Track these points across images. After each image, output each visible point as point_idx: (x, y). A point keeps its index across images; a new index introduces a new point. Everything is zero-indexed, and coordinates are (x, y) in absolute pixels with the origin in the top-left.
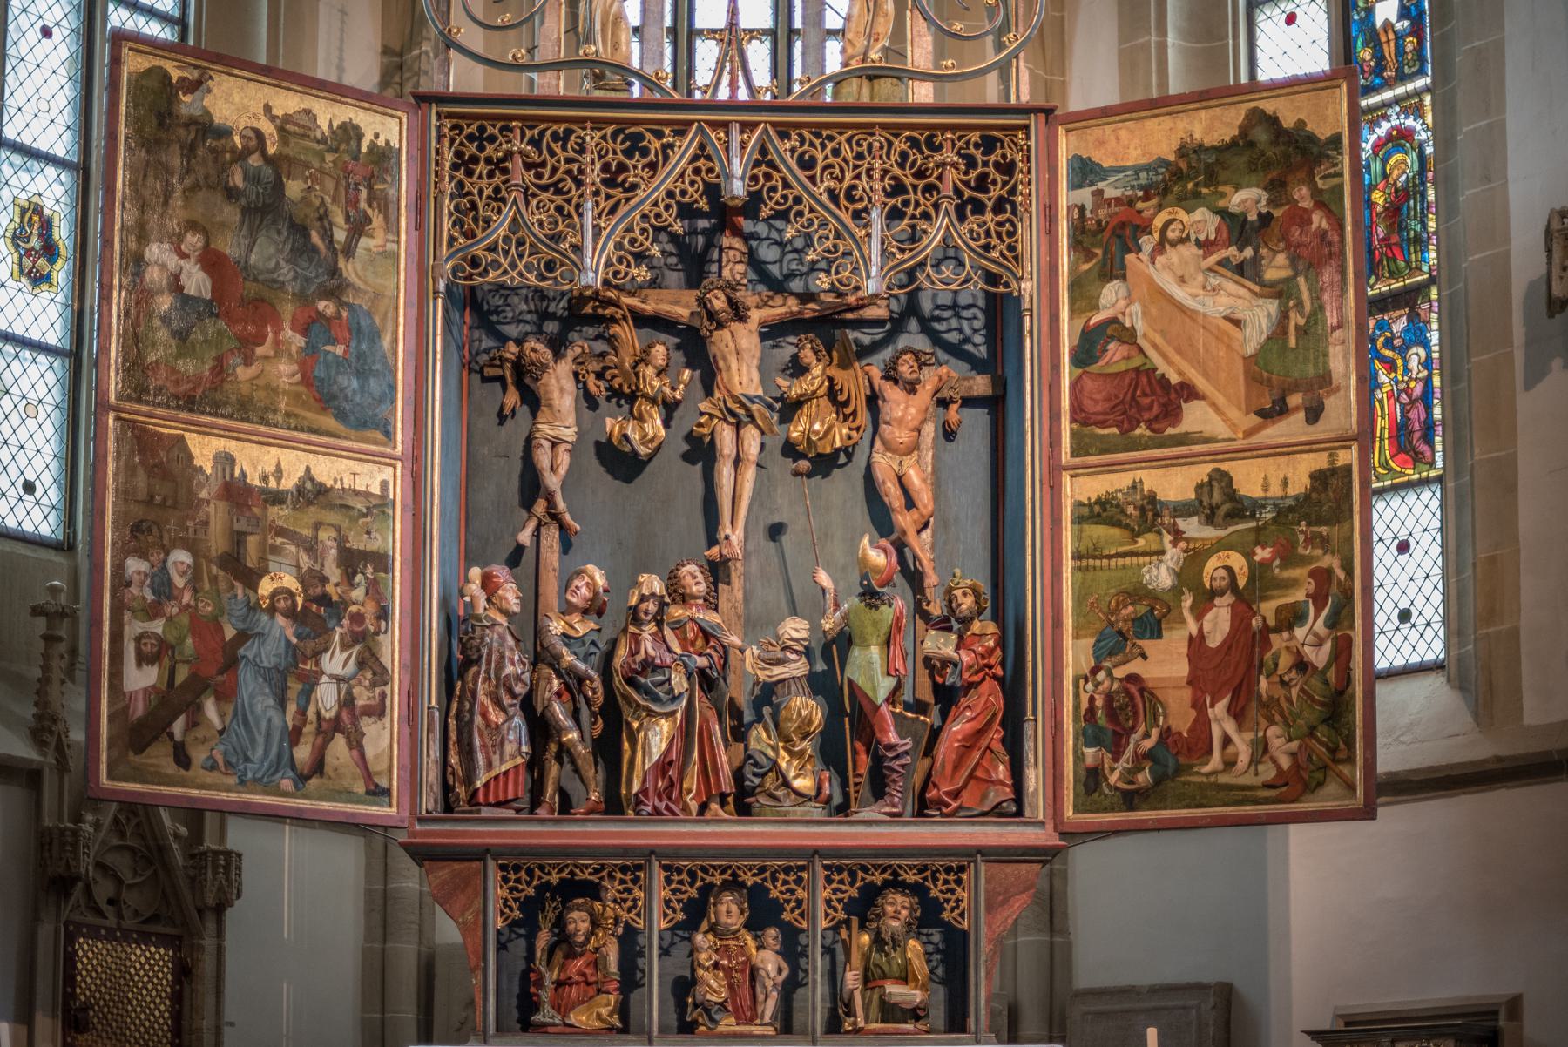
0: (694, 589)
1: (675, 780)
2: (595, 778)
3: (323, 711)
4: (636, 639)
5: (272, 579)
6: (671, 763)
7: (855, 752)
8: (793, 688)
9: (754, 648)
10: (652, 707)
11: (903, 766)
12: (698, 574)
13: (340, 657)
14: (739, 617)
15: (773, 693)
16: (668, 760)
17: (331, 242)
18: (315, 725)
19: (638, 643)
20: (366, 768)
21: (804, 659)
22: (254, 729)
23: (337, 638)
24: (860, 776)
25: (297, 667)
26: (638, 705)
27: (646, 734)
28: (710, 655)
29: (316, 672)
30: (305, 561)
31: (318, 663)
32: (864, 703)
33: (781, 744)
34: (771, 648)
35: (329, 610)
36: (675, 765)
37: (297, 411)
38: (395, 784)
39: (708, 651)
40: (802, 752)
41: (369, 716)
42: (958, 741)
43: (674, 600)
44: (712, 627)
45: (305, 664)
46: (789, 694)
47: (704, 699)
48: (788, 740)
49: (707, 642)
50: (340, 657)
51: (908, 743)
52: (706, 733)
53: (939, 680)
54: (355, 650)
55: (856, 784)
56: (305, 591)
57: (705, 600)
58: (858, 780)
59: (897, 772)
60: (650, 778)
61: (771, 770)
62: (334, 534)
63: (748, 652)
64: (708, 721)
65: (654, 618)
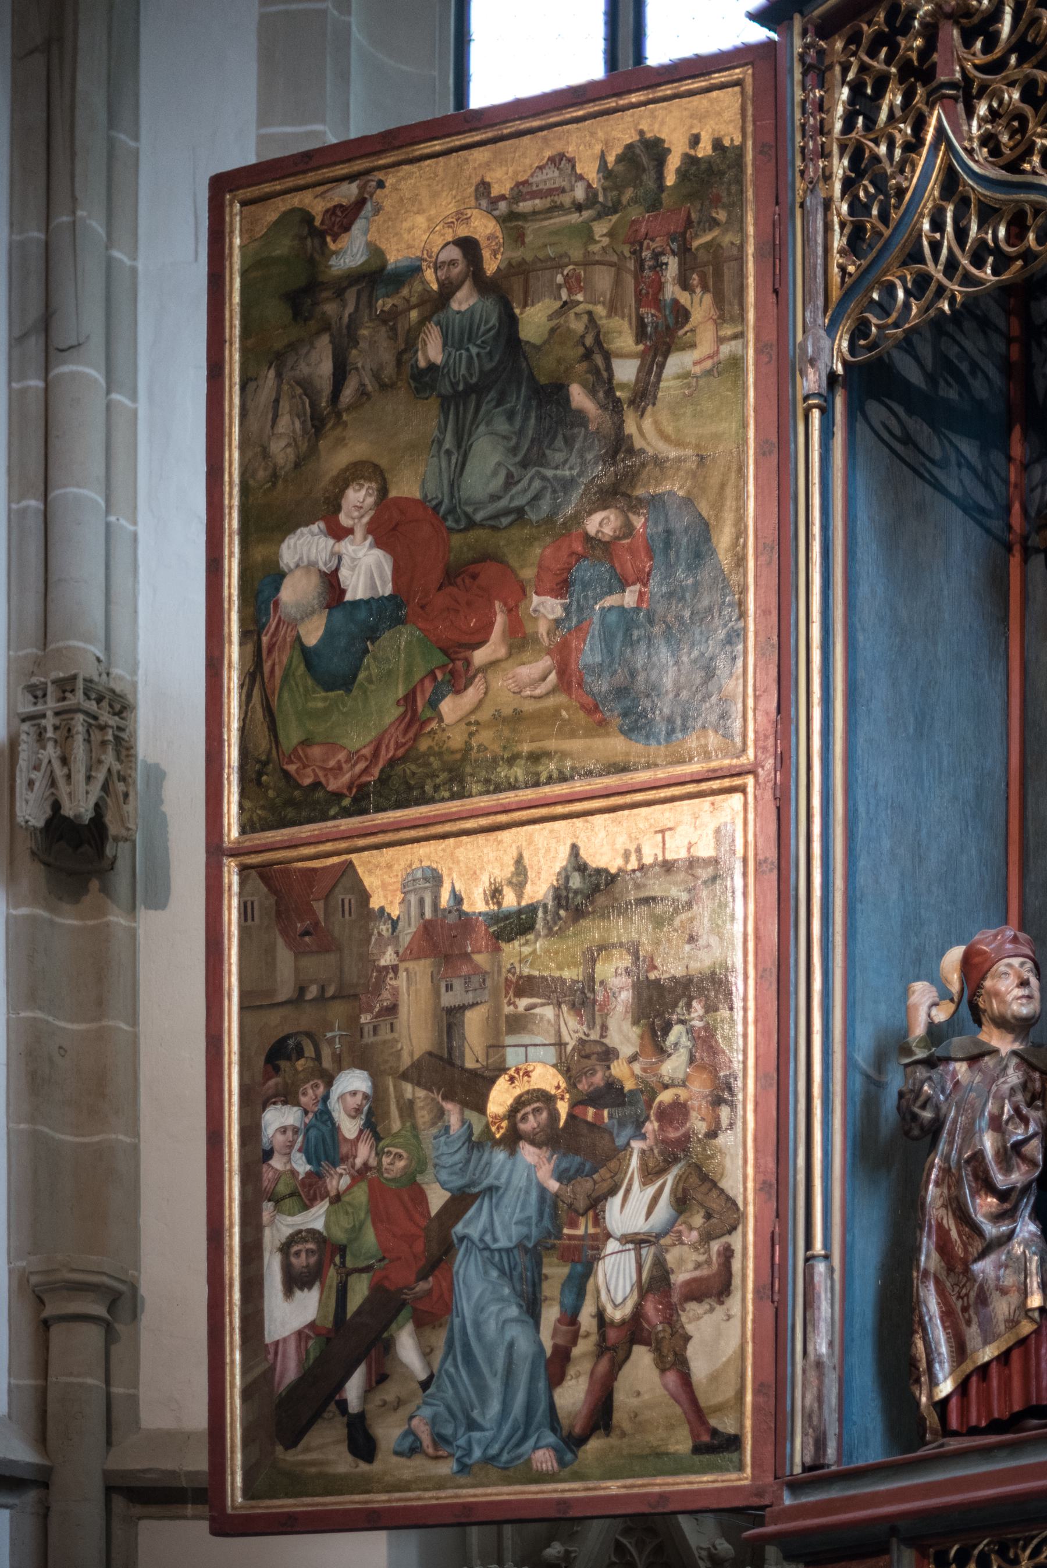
3: (609, 1308)
5: (512, 1079)
13: (640, 1196)
17: (610, 391)
18: (594, 1338)
20: (693, 1401)
22: (485, 1369)
23: (635, 1162)
25: (559, 1235)
29: (595, 1237)
30: (572, 1029)
31: (598, 1220)
35: (618, 1112)
37: (551, 744)
38: (748, 1423)
41: (699, 1299)
45: (574, 1225)
50: (640, 1196)
54: (670, 1178)
56: (572, 1083)
62: (627, 961)
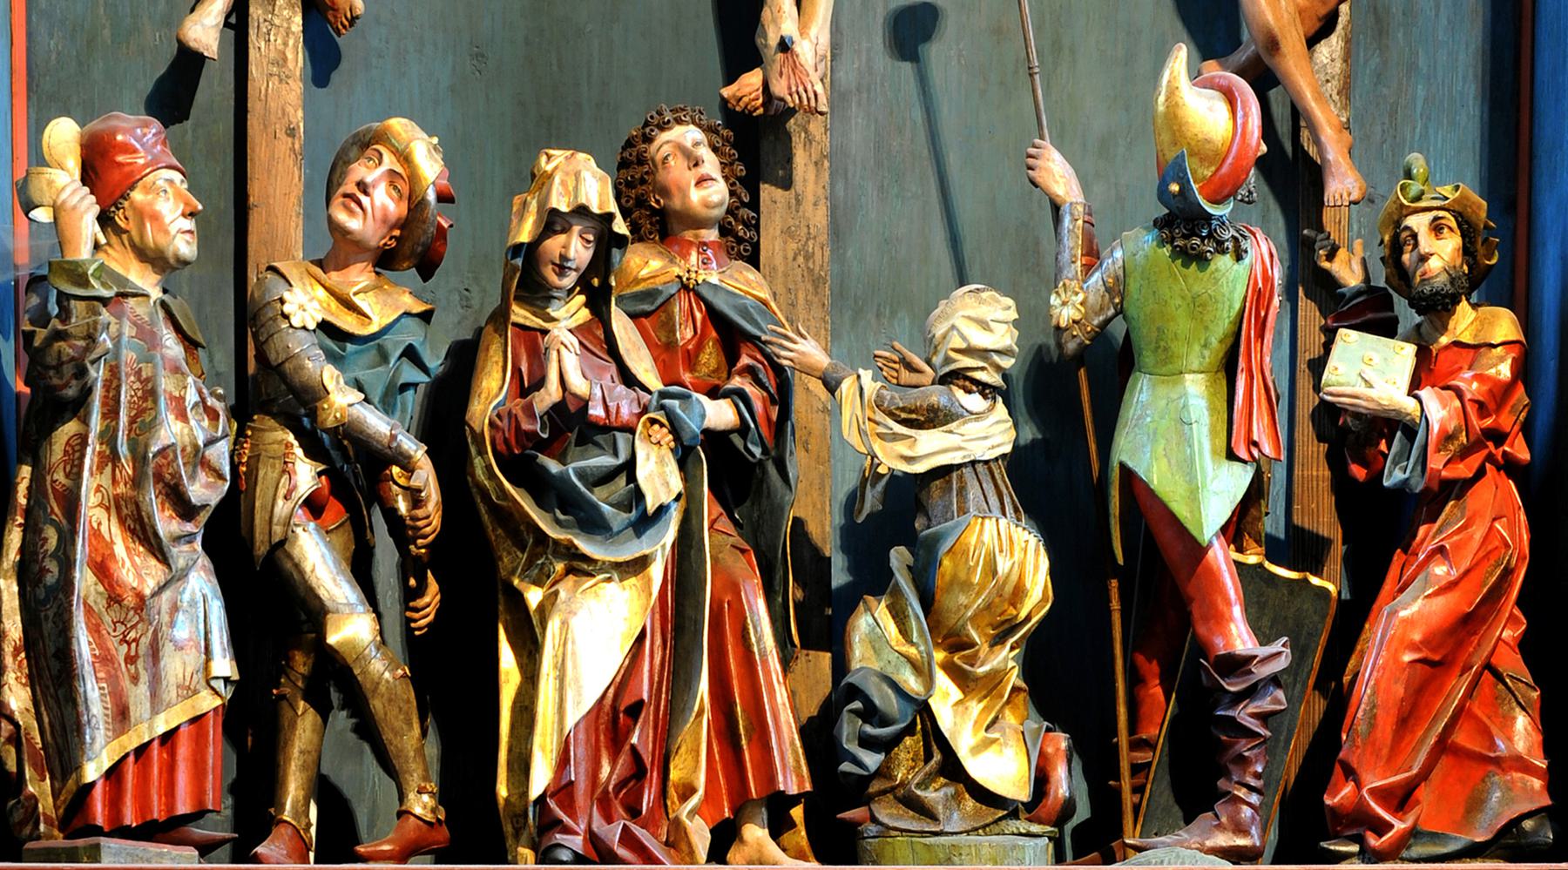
0: (696, 196)
1: (647, 759)
2: (420, 751)
4: (534, 342)
6: (635, 710)
7: (1135, 680)
8: (973, 492)
9: (866, 376)
10: (584, 546)
11: (1264, 717)
12: (705, 153)
14: (817, 282)
15: (920, 507)
16: (627, 701)
19: (538, 357)
21: (1001, 410)
24: (1149, 745)
26: (542, 537)
27: (565, 623)
28: (741, 394)
32: (1165, 536)
33: (939, 656)
34: (906, 376)
36: (648, 714)
39: (737, 382)
40: (996, 679)
42: (1414, 647)
43: (635, 228)
44: (744, 312)
46: (963, 510)
47: (725, 524)
48: (957, 643)
49: (731, 357)
51: (1278, 656)
52: (731, 619)
53: (1359, 472)
55: (1136, 769)
57: (724, 231)
58: (1142, 757)
59: (1253, 735)
60: (578, 753)
61: (909, 730)
63: (847, 387)
64: (735, 589)
65: (583, 284)
